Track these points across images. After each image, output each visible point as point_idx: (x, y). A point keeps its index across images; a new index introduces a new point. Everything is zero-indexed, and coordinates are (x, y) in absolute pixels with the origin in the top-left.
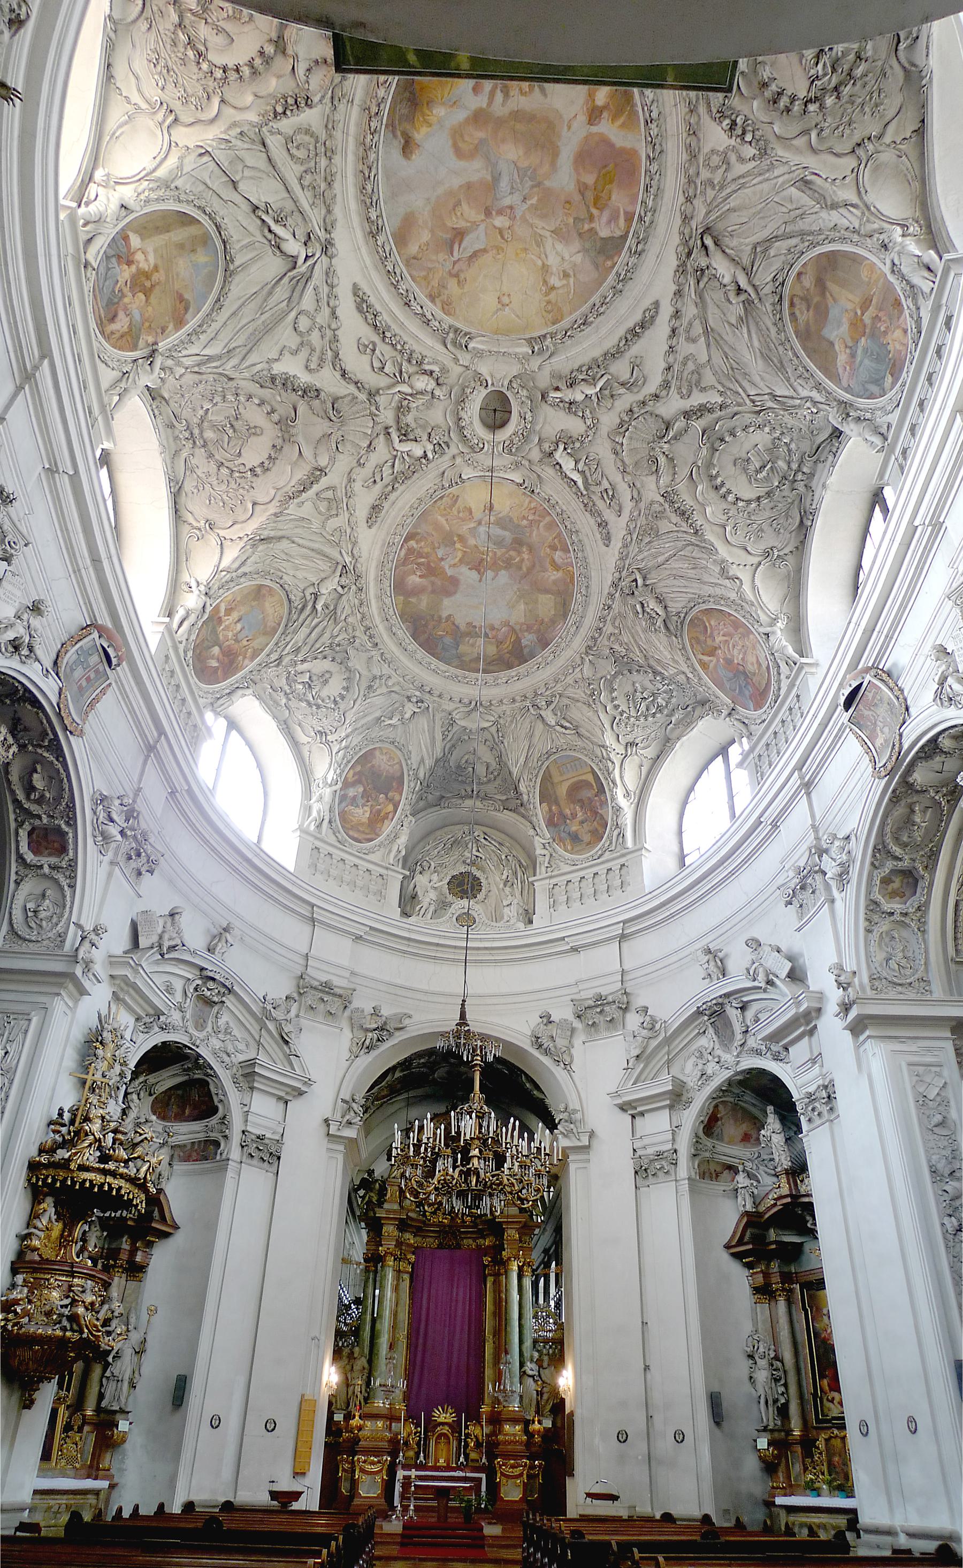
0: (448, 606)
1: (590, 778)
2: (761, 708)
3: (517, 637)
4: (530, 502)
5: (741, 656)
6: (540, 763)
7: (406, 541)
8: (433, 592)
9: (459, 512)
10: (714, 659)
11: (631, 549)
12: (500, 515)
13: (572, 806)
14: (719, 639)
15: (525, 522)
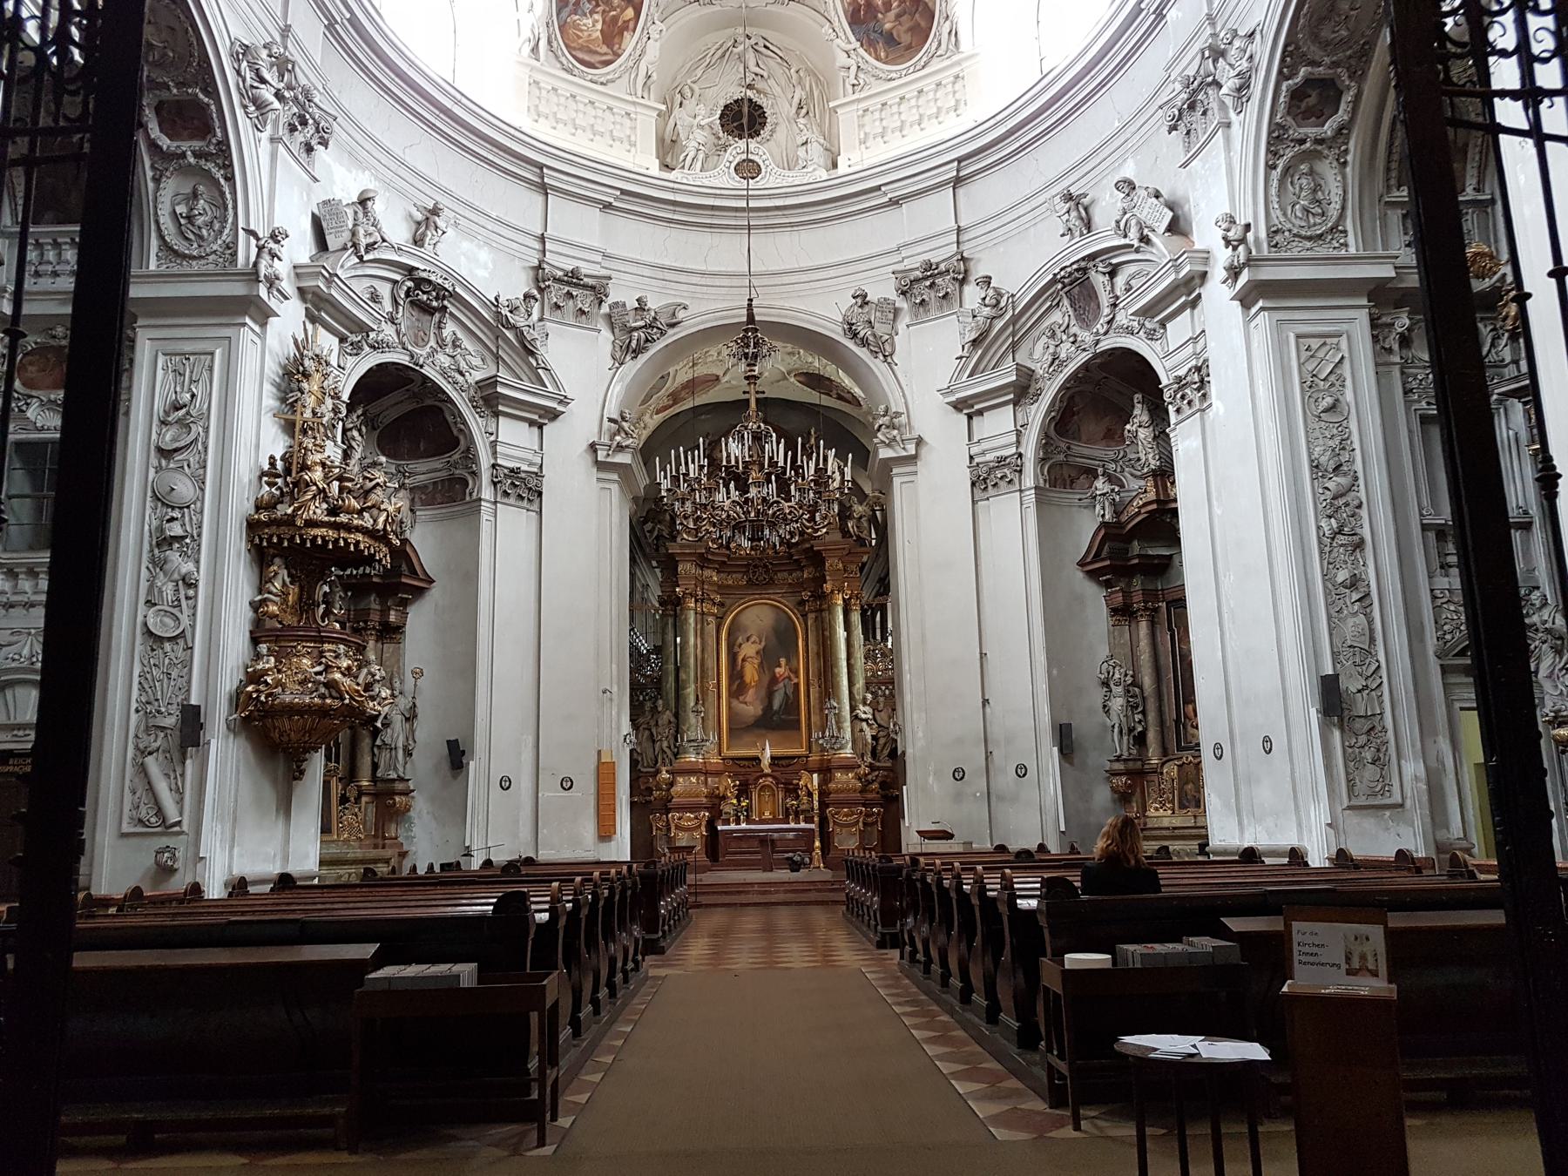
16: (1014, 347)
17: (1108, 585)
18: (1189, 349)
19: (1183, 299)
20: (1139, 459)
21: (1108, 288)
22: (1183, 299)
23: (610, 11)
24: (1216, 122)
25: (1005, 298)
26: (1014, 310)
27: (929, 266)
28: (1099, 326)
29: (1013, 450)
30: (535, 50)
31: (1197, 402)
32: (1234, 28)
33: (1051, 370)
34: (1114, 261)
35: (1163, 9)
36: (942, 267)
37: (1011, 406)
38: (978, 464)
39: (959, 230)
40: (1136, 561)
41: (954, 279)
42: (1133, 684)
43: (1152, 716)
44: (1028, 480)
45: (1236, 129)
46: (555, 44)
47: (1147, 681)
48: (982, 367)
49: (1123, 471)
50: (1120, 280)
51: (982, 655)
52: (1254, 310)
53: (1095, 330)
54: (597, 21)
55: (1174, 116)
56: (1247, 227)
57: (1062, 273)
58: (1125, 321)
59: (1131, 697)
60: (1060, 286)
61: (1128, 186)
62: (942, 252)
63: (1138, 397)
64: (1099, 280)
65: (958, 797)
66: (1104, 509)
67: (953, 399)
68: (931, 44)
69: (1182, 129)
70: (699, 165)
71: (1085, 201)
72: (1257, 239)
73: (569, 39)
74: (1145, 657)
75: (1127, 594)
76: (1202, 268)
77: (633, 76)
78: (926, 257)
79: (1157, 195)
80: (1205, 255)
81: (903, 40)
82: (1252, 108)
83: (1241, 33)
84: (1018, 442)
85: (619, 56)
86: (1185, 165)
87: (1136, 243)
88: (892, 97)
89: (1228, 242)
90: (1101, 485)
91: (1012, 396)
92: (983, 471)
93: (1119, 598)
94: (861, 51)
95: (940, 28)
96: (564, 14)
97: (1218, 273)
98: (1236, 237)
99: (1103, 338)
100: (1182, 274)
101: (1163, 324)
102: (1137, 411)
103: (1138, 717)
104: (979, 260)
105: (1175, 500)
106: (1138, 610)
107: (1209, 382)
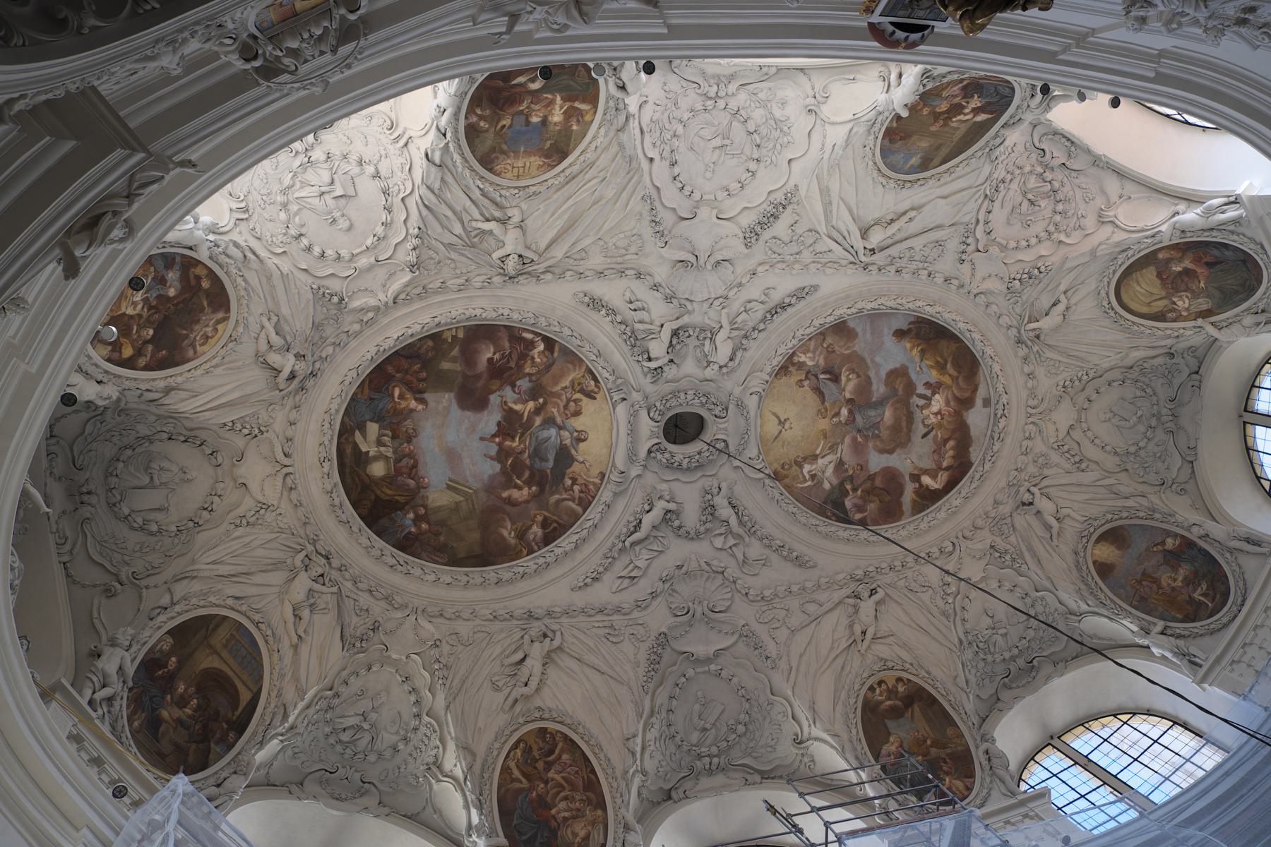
0: (443, 401)
1: (245, 696)
3: (406, 503)
4: (594, 484)
5: (566, 814)
6: (230, 602)
9: (576, 401)
10: (525, 784)
11: (581, 618)
12: (573, 452)
13: (192, 690)
15: (569, 482)
23: (138, 325)
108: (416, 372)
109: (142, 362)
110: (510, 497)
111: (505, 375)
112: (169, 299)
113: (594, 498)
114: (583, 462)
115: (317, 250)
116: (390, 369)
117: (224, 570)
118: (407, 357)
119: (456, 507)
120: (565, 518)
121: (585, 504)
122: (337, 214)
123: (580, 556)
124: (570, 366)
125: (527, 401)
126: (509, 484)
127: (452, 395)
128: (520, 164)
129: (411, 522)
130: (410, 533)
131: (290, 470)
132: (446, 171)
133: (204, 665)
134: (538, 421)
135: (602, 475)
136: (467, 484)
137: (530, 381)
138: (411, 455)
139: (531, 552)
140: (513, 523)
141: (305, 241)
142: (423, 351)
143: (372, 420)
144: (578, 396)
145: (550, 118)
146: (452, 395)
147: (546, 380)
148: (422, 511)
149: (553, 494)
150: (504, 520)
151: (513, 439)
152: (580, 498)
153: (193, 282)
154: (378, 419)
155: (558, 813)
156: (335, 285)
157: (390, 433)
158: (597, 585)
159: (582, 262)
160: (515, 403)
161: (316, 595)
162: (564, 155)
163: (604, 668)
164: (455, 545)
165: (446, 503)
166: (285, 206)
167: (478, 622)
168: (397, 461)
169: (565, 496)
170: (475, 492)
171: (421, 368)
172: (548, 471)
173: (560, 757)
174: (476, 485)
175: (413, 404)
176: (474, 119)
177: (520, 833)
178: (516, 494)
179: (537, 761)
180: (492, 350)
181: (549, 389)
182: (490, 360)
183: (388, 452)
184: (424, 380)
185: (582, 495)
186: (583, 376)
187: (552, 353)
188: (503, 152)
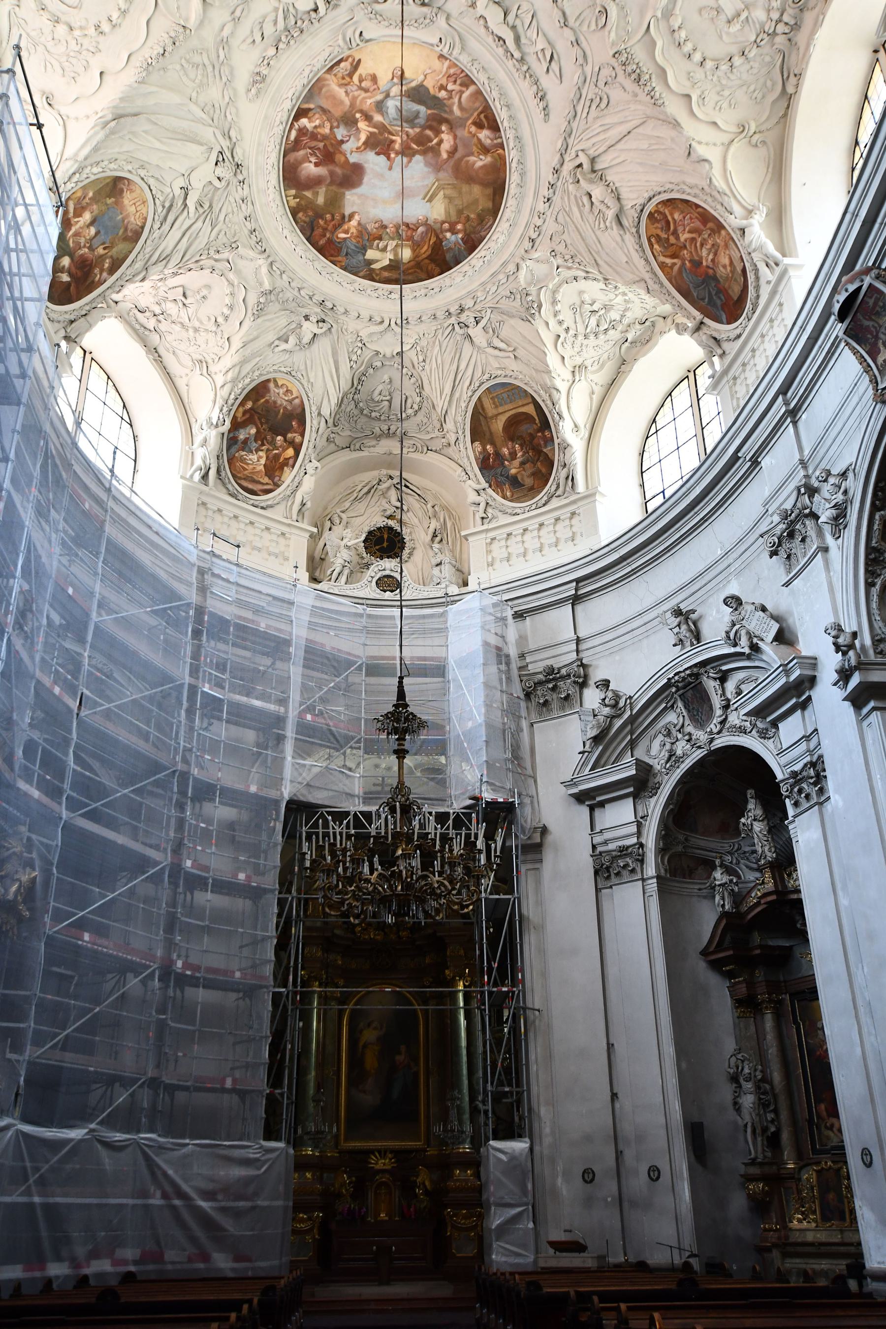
0: (352, 200)
1: (530, 409)
2: (736, 320)
3: (437, 237)
4: (449, 68)
5: (711, 257)
6: (470, 394)
7: (297, 118)
8: (332, 183)
9: (361, 81)
12: (413, 84)
14: (684, 236)
16: (632, 745)
17: (729, 975)
18: (803, 746)
19: (794, 701)
20: (754, 852)
21: (720, 692)
22: (794, 701)
24: (815, 547)
25: (623, 700)
26: (631, 710)
27: (550, 670)
28: (712, 726)
29: (634, 840)
30: (205, 477)
31: (814, 795)
32: (828, 468)
33: (668, 766)
34: (724, 668)
35: (758, 457)
36: (564, 672)
37: (631, 800)
38: (601, 853)
39: (578, 641)
40: (758, 952)
41: (575, 682)
42: (764, 1080)
43: (784, 1115)
44: (649, 869)
45: (834, 553)
46: (223, 474)
47: (777, 1077)
48: (602, 762)
49: (738, 863)
50: (730, 686)
51: (610, 1046)
52: (865, 711)
53: (708, 730)
54: (261, 457)
55: (774, 543)
56: (854, 635)
57: (676, 678)
58: (737, 722)
59: (763, 1094)
60: (674, 690)
61: (734, 602)
62: (565, 657)
63: (750, 792)
64: (711, 685)
65: (588, 1202)
66: (723, 899)
67: (575, 790)
68: (550, 486)
69: (783, 554)
70: (343, 579)
71: (693, 616)
72: (863, 647)
73: (235, 470)
74: (772, 1051)
75: (750, 984)
76: (809, 673)
77: (289, 503)
78: (549, 662)
79: (764, 609)
80: (813, 661)
81: (526, 483)
82: (849, 534)
83: (834, 472)
84: (639, 834)
85: (279, 486)
86: (787, 584)
87: (747, 650)
88: (517, 529)
89: (838, 648)
90: (719, 876)
91: (631, 789)
92: (606, 860)
93: (743, 990)
94: (490, 491)
95: (558, 474)
96: (233, 450)
97: (828, 673)
98: (846, 643)
99: (717, 736)
100: (793, 678)
101: (775, 724)
102: (751, 805)
103: (770, 1116)
104: (597, 667)
105: (798, 891)
106: (763, 1001)
107: (825, 777)
108: (325, 223)
109: (298, 439)
110: (448, 152)
111: (331, 150)
112: (258, 432)
113: (463, 71)
114: (425, 76)
115: (226, 311)
116: (322, 242)
117: (448, 390)
118: (313, 230)
119: (449, 199)
120: (477, 104)
121: (468, 82)
122: (198, 297)
123: (517, 103)
124: (324, 90)
125: (358, 129)
126: (435, 151)
127: (347, 193)
128: (132, 209)
129: (453, 237)
130: (462, 239)
131: (393, 323)
132: (149, 263)
133: (501, 429)
134: (378, 118)
135: (441, 57)
136: (430, 185)
137: (338, 127)
138: (397, 227)
139: (502, 146)
140: (472, 154)
141: (220, 320)
142: (307, 220)
143: (364, 255)
144: (356, 78)
145: (89, 222)
146: (347, 193)
147: (337, 112)
148: (446, 226)
149: (452, 112)
150: (468, 161)
151: (393, 142)
152: (461, 85)
153: (247, 416)
154: (364, 249)
155: (707, 261)
156: (252, 299)
157: (377, 241)
158: (549, 97)
159: (217, 106)
160: (359, 139)
161: (488, 325)
162: (117, 180)
163: (624, 129)
164: (480, 207)
165: (443, 206)
166: (196, 330)
167: (548, 213)
168: (400, 237)
169: (456, 100)
170: (437, 180)
171: (322, 219)
172: (429, 112)
173: (674, 219)
174: (431, 179)
175: (354, 223)
176: (105, 274)
177: (703, 299)
178: (446, 146)
179: (668, 239)
180: (306, 165)
181: (347, 108)
182: (316, 165)
183: (392, 244)
184: (333, 216)
185: (458, 82)
186: (335, 75)
187: (310, 110)
188: (126, 229)
